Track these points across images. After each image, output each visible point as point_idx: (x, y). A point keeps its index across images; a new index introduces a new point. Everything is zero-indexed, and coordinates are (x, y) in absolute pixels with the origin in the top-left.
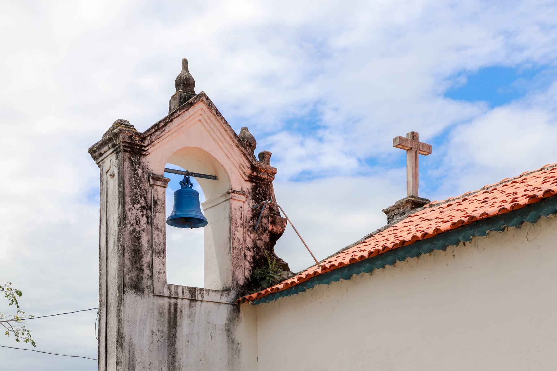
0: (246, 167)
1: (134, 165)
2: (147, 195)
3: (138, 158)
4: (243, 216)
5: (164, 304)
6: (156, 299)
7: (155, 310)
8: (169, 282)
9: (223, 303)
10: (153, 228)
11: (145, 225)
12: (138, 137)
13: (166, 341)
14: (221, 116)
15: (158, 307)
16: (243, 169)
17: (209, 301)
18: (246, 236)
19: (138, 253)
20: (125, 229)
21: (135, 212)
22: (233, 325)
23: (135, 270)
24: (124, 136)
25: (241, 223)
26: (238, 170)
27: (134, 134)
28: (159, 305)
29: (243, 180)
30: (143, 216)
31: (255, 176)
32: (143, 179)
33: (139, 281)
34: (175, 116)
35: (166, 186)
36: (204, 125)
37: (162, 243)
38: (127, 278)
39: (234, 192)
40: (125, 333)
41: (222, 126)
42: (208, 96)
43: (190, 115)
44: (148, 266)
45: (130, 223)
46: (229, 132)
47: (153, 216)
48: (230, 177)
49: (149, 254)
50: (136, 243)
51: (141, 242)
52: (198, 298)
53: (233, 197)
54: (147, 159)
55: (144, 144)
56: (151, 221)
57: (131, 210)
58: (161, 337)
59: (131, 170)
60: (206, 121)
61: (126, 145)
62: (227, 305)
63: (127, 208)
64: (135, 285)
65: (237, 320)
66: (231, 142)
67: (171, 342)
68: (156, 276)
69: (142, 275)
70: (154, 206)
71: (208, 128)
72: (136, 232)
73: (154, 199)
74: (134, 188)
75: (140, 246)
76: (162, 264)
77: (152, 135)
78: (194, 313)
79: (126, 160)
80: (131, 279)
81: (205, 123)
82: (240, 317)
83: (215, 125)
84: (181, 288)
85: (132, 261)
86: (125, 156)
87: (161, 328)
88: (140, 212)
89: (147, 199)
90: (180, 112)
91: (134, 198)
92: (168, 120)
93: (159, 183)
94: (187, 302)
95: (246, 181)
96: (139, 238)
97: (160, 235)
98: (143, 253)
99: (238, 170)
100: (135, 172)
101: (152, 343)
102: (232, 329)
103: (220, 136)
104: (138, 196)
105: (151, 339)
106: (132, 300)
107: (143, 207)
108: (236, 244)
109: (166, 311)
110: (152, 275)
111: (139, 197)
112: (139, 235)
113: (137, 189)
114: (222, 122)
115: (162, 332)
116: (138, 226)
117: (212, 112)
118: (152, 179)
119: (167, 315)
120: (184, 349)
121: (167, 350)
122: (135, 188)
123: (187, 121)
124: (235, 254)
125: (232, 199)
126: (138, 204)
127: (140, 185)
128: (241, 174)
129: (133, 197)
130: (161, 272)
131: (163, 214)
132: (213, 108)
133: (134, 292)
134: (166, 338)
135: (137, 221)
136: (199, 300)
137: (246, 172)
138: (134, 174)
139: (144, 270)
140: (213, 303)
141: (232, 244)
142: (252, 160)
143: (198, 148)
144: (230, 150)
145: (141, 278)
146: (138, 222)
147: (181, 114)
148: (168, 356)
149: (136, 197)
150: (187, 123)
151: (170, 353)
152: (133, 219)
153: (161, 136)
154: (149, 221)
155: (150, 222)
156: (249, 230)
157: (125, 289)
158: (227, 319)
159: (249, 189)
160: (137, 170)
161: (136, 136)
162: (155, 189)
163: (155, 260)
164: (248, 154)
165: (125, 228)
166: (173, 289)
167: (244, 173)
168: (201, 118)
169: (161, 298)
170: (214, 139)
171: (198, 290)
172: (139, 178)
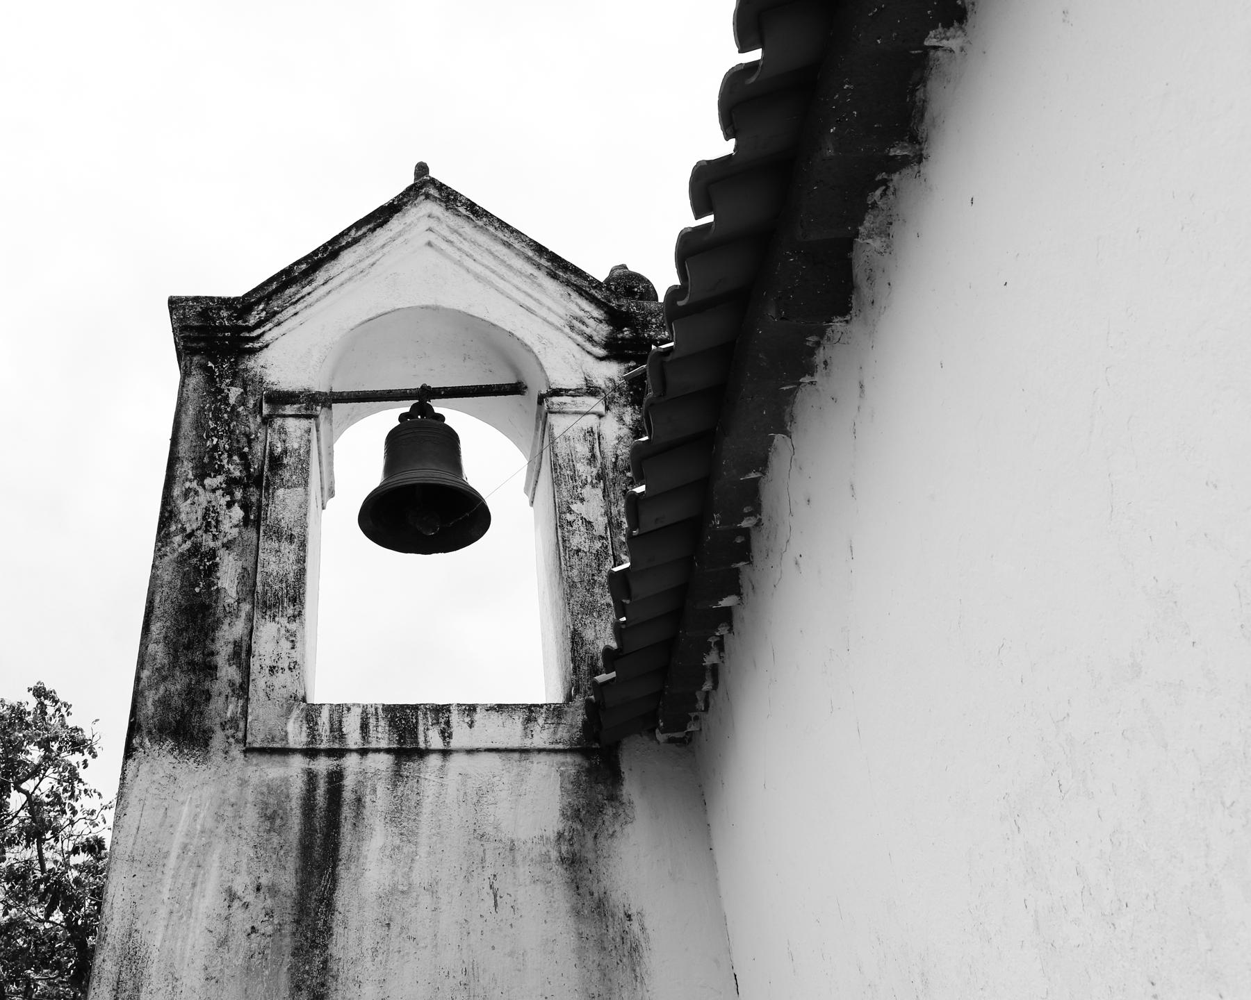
1: (218, 380)
2: (250, 448)
3: (231, 362)
5: (286, 781)
6: (256, 765)
7: (248, 805)
8: (315, 699)
12: (227, 309)
13: (288, 929)
20: (163, 549)
21: (203, 498)
23: (182, 672)
24: (184, 314)
27: (214, 302)
28: (268, 786)
35: (314, 413)
37: (292, 574)
45: (184, 530)
49: (243, 614)
50: (198, 586)
51: (216, 581)
55: (246, 322)
58: (267, 914)
61: (189, 336)
63: (177, 492)
67: (309, 935)
68: (260, 681)
72: (201, 555)
75: (210, 594)
76: (287, 639)
77: (274, 298)
84: (357, 712)
86: (191, 363)
87: (270, 875)
88: (223, 496)
89: (250, 457)
91: (206, 460)
93: (289, 409)
97: (288, 550)
100: (219, 397)
101: (223, 942)
104: (220, 456)
105: (220, 927)
107: (232, 483)
109: (295, 805)
111: (226, 455)
112: (211, 562)
113: (220, 437)
115: (273, 890)
118: (267, 402)
119: (295, 822)
121: (289, 969)
122: (212, 436)
127: (232, 425)
129: (201, 458)
130: (281, 666)
131: (300, 489)
134: (288, 918)
135: (209, 524)
146: (213, 523)
149: (212, 458)
151: (304, 981)
152: (195, 517)
153: (303, 297)
154: (252, 517)
155: (254, 518)
160: (226, 391)
161: (220, 309)
162: (277, 428)
163: (261, 628)
165: (163, 546)
166: (324, 718)
169: (277, 758)
172: (229, 409)
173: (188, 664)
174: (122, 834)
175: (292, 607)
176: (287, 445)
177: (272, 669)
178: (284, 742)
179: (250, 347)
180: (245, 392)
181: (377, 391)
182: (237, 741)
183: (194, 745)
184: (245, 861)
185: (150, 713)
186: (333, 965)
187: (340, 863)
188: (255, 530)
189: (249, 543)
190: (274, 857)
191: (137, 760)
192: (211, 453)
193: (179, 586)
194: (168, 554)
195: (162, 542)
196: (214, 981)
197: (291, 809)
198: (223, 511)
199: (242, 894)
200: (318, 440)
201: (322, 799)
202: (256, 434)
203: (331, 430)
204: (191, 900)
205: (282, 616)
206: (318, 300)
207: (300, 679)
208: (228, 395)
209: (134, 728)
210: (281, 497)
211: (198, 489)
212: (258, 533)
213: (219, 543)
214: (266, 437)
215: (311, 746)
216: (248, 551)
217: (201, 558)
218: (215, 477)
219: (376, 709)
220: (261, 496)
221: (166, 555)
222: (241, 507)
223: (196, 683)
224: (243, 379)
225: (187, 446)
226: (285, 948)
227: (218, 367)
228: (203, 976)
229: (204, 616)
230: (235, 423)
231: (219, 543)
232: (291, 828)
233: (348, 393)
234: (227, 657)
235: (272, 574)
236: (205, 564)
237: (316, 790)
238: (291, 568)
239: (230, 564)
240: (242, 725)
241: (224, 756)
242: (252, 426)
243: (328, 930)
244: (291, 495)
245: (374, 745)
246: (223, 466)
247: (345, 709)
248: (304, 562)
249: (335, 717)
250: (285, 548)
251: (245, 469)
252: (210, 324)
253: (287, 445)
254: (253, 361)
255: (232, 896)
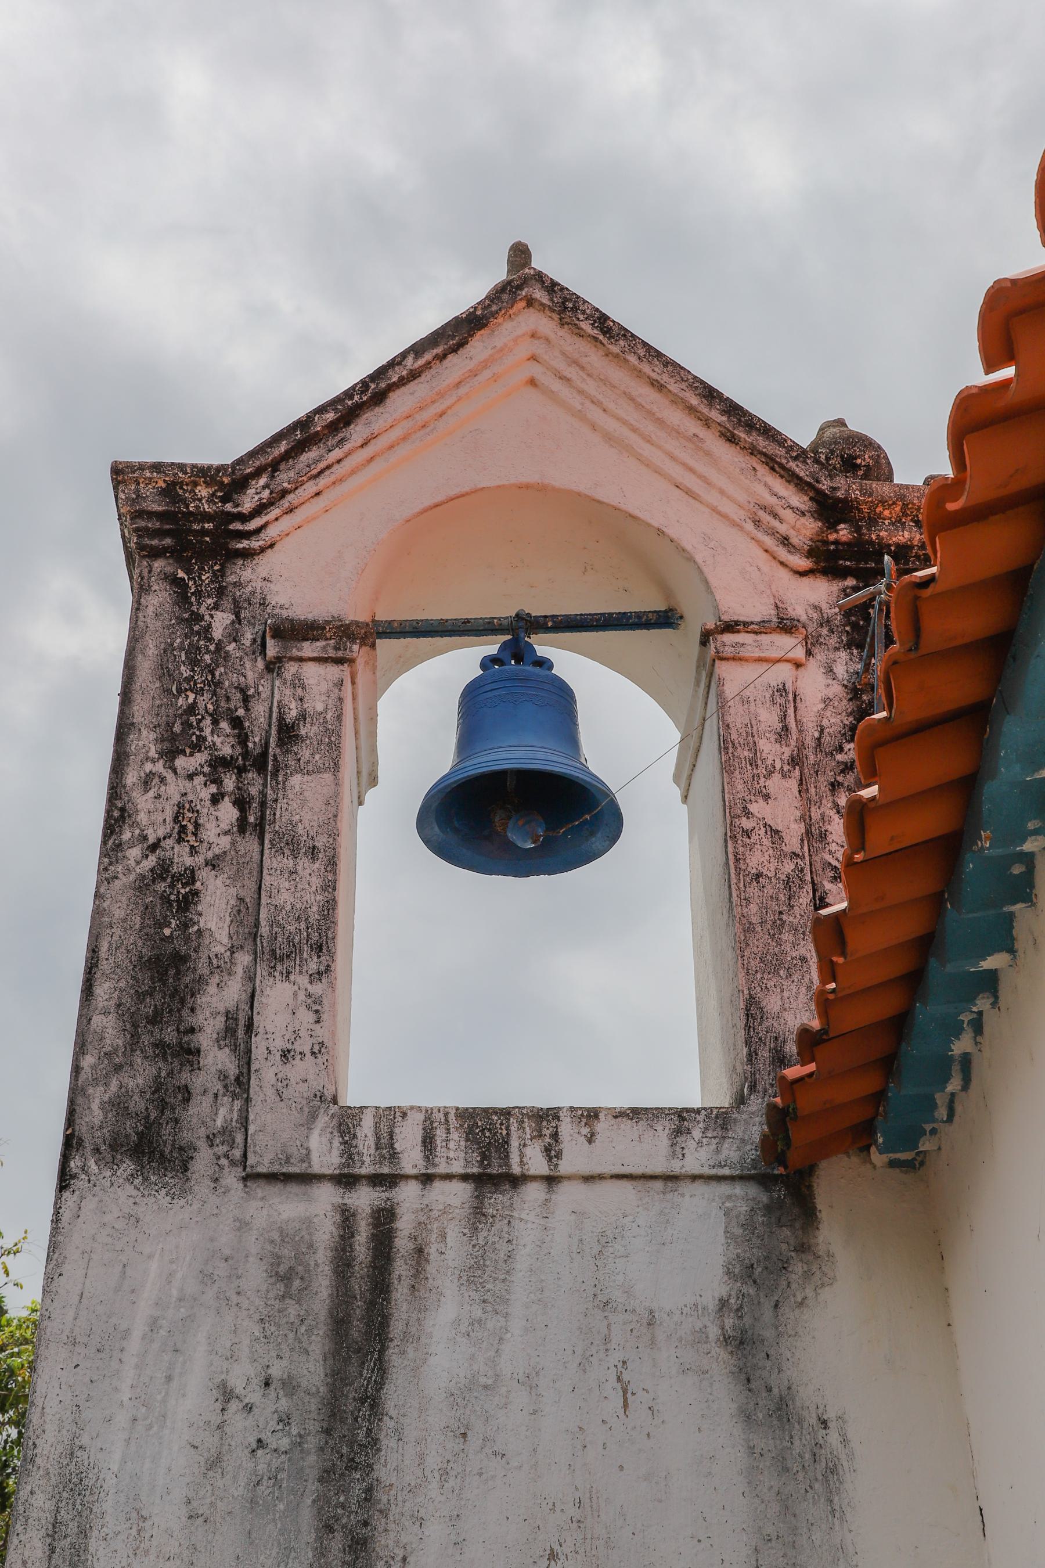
0: (789, 511)
1: (193, 599)
2: (247, 709)
4: (792, 725)
5: (308, 1222)
6: (263, 1198)
7: (251, 1259)
9: (695, 1178)
10: (267, 844)
11: (225, 841)
12: (208, 485)
13: (312, 1443)
14: (626, 334)
15: (272, 1242)
16: (776, 523)
17: (601, 1177)
18: (823, 815)
19: (172, 972)
20: (112, 868)
21: (174, 788)
22: (776, 1306)
24: (137, 491)
25: (786, 756)
26: (748, 534)
27: (185, 473)
28: (281, 1231)
29: (783, 574)
30: (215, 800)
31: (847, 544)
32: (231, 647)
33: (167, 1113)
34: (395, 379)
35: (348, 654)
36: (551, 395)
37: (315, 909)
38: (95, 1106)
39: (730, 627)
40: (43, 1414)
41: (639, 374)
42: (556, 279)
43: (471, 365)
44: (229, 1031)
45: (145, 838)
46: (673, 387)
47: (269, 792)
48: (705, 570)
49: (239, 970)
50: (169, 925)
51: (196, 918)
52: (522, 1163)
53: (728, 651)
54: (260, 569)
55: (238, 506)
56: (263, 817)
57: (156, 781)
58: (280, 1420)
59: (173, 621)
60: (560, 378)
61: (147, 529)
62: (725, 1188)
63: (131, 778)
64: (141, 1135)
65: (798, 1268)
66: (693, 427)
67: (345, 1450)
69: (185, 1077)
70: (278, 751)
71: (576, 402)
72: (173, 877)
73: (281, 719)
74: (180, 691)
75: (187, 940)
76: (308, 1007)
78: (502, 1255)
79: (155, 587)
80: (118, 1106)
81: (556, 386)
82: (821, 1250)
83: (605, 381)
85: (132, 1015)
86: (150, 572)
87: (284, 1363)
88: (205, 785)
89: (247, 724)
90: (416, 358)
91: (177, 728)
92: (356, 398)
93: (309, 649)
94: (458, 1194)
95: (802, 574)
96: (188, 902)
97: (308, 871)
98: (202, 967)
99: (748, 534)
100: (196, 628)
102: (769, 1334)
103: (633, 416)
104: (199, 721)
106: (108, 1218)
107: (219, 764)
108: (758, 859)
109: (322, 1259)
110: (245, 1071)
111: (208, 721)
112: (187, 890)
113: (199, 692)
114: (633, 359)
115: (290, 1385)
116: (187, 849)
117: (580, 334)
118: (273, 637)
119: (323, 1284)
120: (435, 1484)
121: (314, 1501)
122: (186, 690)
123: (463, 390)
124: (753, 908)
125: (722, 659)
126: (198, 755)
127: (217, 673)
128: (766, 551)
129: (169, 726)
130: (299, 1049)
131: (328, 777)
132: (581, 317)
133: (129, 1172)
134: (313, 1426)
135: (183, 829)
136: (532, 1172)
137: (792, 534)
138: (186, 636)
139: (199, 1051)
140: (627, 1185)
141: (737, 860)
142: (812, 475)
143: (527, 486)
144: (691, 462)
145: (180, 1097)
146: (191, 828)
147: (428, 365)
148: (319, 1539)
149: (187, 725)
150: (459, 399)
152: (161, 819)
153: (328, 467)
154: (251, 819)
156: (840, 784)
157: (74, 1164)
158: (728, 1273)
159: (824, 606)
160: (207, 618)
161: (196, 484)
162: (289, 678)
163: (268, 991)
164: (786, 453)
165: (111, 864)
167: (785, 541)
168: (536, 370)
169: (294, 1188)
170: (609, 438)
171: (522, 1122)
172: (212, 648)
173: (156, 1045)
174: (55, 1304)
175: (315, 959)
176: (305, 706)
177: (285, 1055)
178: (305, 1165)
179: (244, 548)
180: (238, 619)
181: (447, 621)
182: (233, 1163)
183: (166, 1169)
184: (246, 1342)
185: (97, 1122)
186: (381, 1496)
187: (392, 1345)
188: (256, 841)
189: (248, 859)
190: (291, 1335)
191: (77, 1193)
192: (185, 717)
193: (137, 927)
194: (120, 876)
195: (110, 857)
196: (201, 1520)
197: (317, 1265)
198: (205, 810)
199: (243, 1392)
200: (354, 698)
201: (363, 1249)
202: (256, 687)
203: (375, 682)
204: (164, 1401)
205: (301, 973)
206: (353, 472)
207: (329, 1068)
208: (210, 625)
209: (71, 1144)
210: (297, 788)
211: (165, 774)
212: (262, 844)
213: (200, 860)
214: (273, 694)
215: (346, 1171)
216: (246, 871)
217: (172, 882)
218: (192, 755)
219: (446, 1115)
220: (265, 785)
221: (117, 878)
222: (234, 803)
223: (168, 1074)
224: (234, 599)
225: (146, 705)
226: (307, 1471)
227: (194, 579)
228: (184, 1512)
229: (178, 972)
230: (222, 669)
231: (200, 860)
232: (316, 1293)
233: (401, 623)
234: (215, 1036)
235: (283, 908)
236: (178, 892)
237: (353, 1236)
238: (314, 900)
239: (218, 892)
240: (239, 1138)
241: (213, 1185)
242: (250, 675)
243: (373, 1444)
244: (312, 785)
245: (442, 1169)
246: (205, 739)
247: (398, 1114)
248: (334, 889)
249: (384, 1126)
250: (304, 868)
251: (239, 743)
252: (179, 507)
253: (305, 706)
254: (250, 570)
255: (227, 1394)
